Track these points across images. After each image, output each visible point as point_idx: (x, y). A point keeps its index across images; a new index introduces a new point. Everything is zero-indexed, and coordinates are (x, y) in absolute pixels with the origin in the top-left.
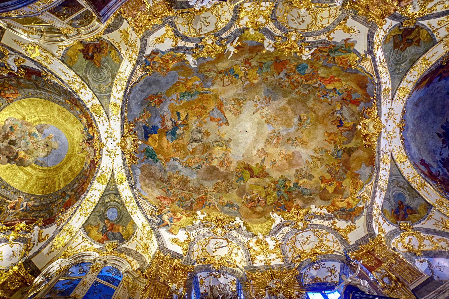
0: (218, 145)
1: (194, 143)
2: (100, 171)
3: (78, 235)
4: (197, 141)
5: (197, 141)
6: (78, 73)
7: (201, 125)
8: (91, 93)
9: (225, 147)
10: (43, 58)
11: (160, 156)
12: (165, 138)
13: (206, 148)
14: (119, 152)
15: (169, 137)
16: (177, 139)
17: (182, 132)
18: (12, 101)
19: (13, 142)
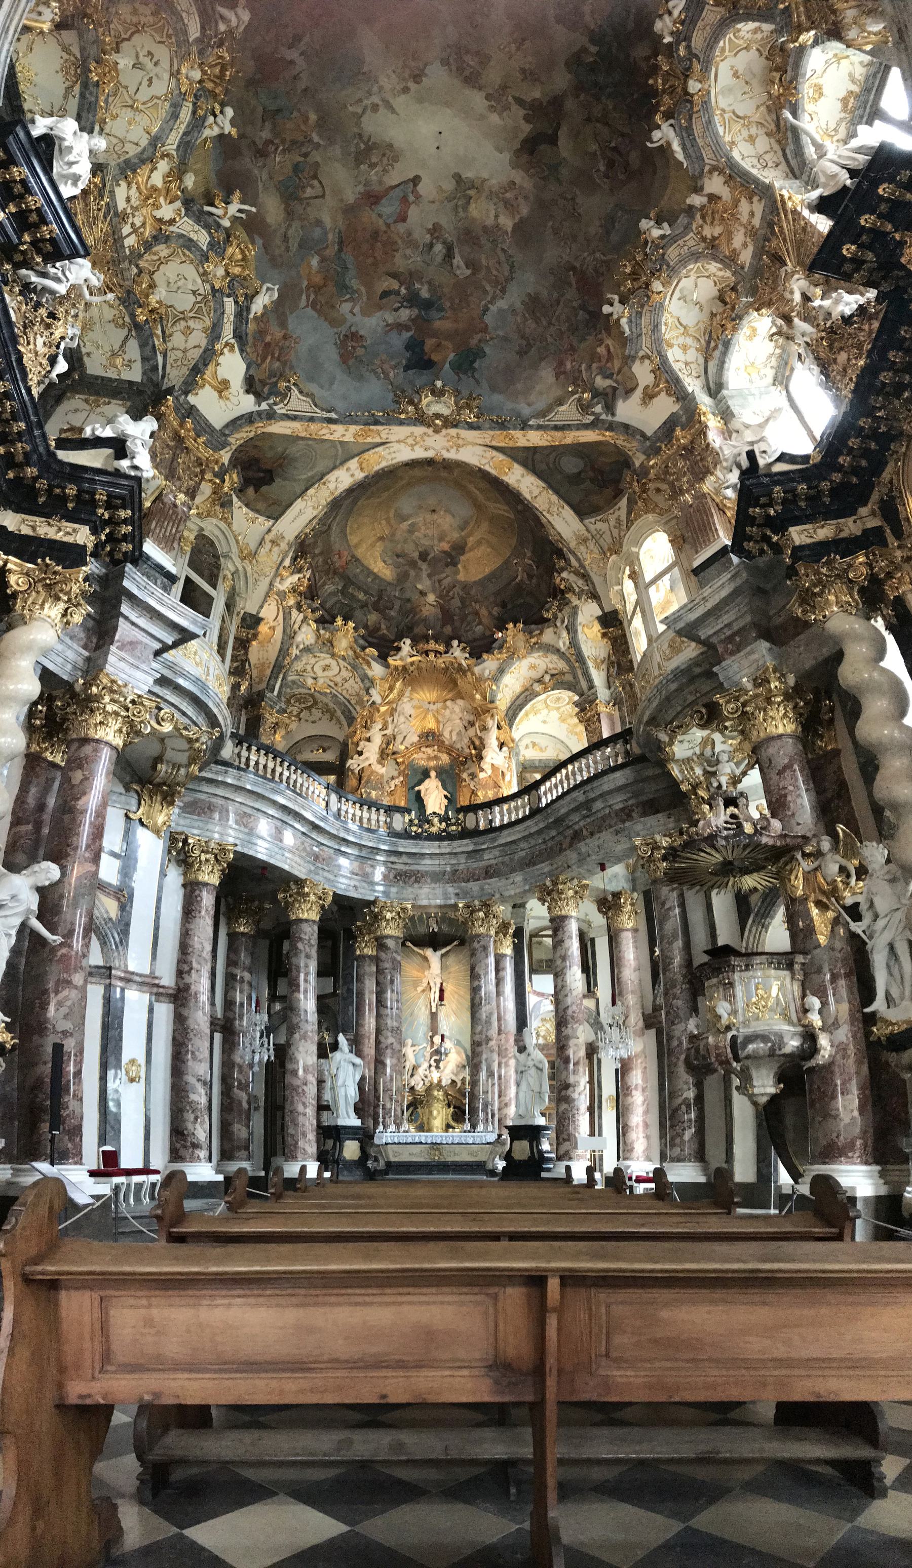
0: (465, 208)
1: (455, 262)
4: (449, 255)
5: (449, 255)
7: (411, 243)
9: (472, 192)
10: (276, 549)
11: (473, 342)
12: (437, 324)
13: (470, 236)
14: (453, 432)
15: (434, 314)
16: (440, 298)
17: (426, 287)
18: (353, 556)
19: (423, 556)
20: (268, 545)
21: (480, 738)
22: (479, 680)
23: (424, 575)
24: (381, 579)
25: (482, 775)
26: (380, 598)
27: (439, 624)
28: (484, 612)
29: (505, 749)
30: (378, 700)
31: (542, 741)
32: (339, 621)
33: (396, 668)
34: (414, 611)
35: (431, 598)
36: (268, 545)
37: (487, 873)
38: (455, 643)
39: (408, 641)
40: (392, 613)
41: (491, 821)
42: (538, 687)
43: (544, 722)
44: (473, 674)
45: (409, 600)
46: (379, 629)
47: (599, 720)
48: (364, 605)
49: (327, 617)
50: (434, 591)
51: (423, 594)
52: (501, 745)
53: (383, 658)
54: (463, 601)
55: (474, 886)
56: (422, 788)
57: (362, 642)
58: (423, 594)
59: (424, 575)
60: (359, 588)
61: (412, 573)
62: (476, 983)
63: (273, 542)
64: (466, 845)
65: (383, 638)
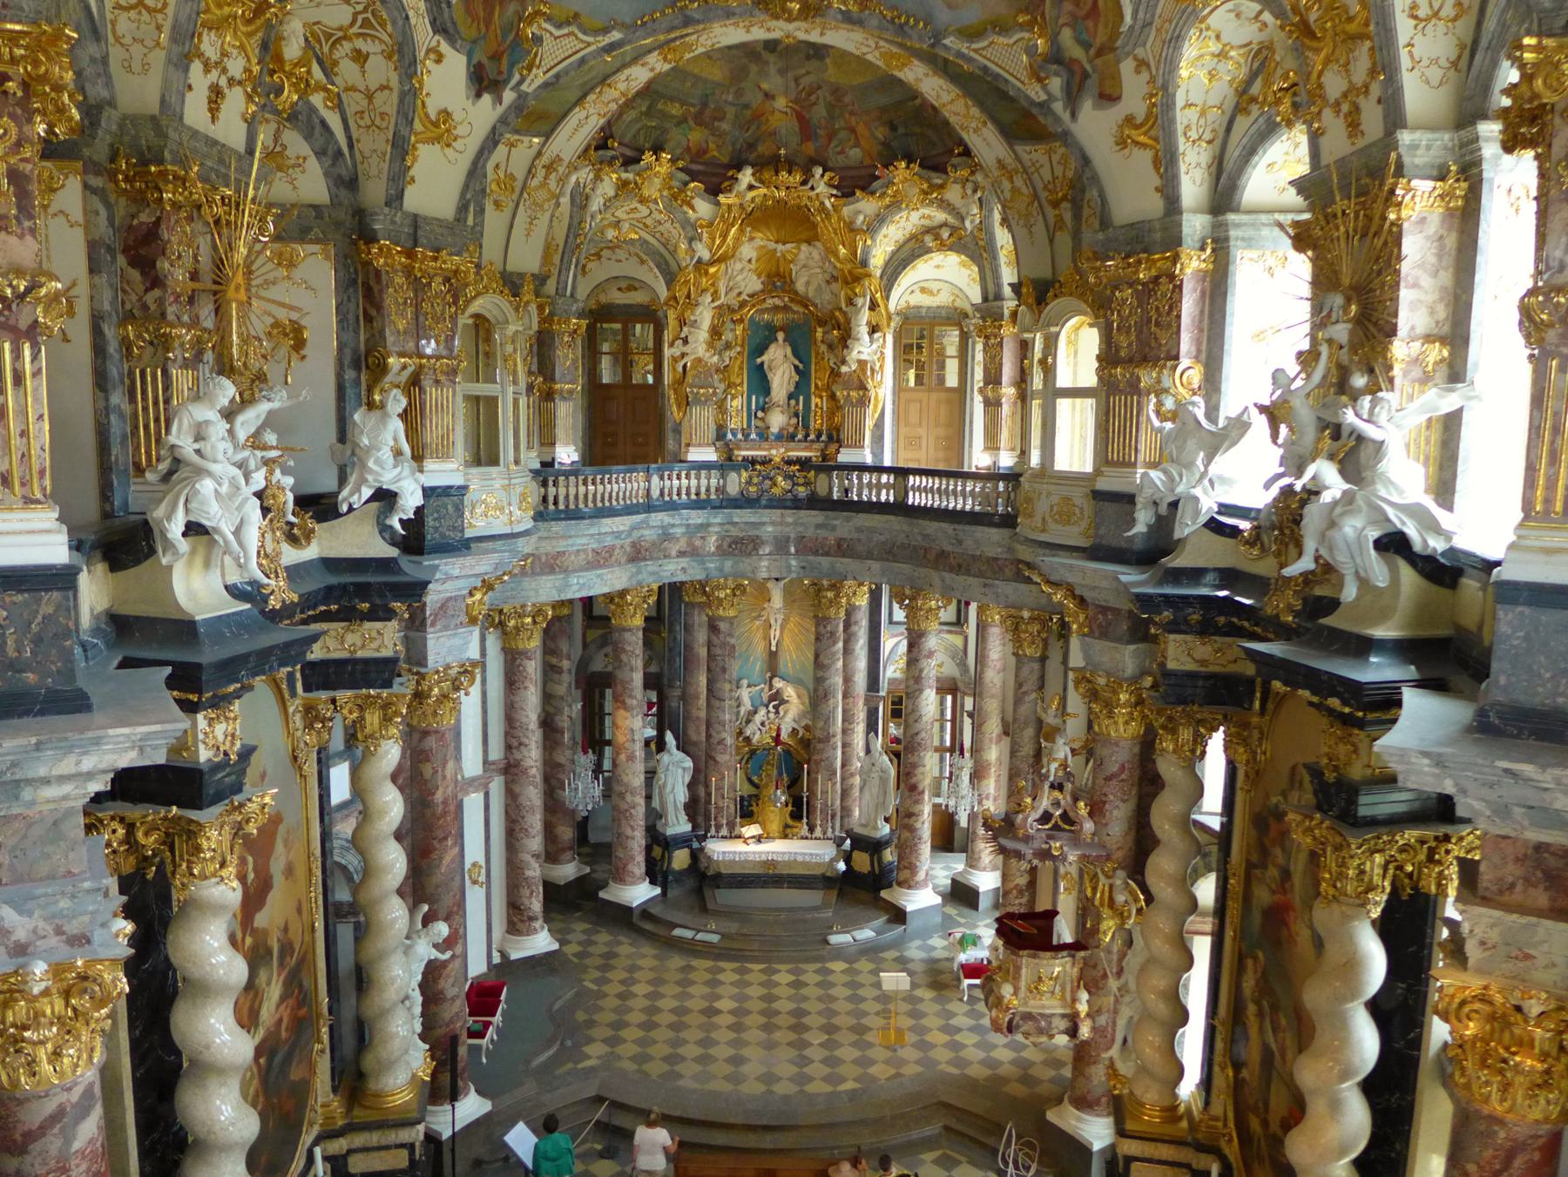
2: (869, 57)
3: (1025, 157)
6: (573, 99)
8: (627, 72)
20: (541, 173)
21: (845, 314)
22: (851, 228)
23: (772, 69)
24: (705, 81)
25: (844, 369)
26: (705, 105)
27: (795, 140)
28: (861, 129)
29: (876, 335)
30: (706, 255)
31: (934, 286)
32: (648, 157)
33: (729, 206)
34: (758, 117)
35: (781, 103)
36: (541, 173)
37: (839, 546)
38: (818, 171)
39: (748, 171)
40: (725, 126)
41: (846, 491)
42: (929, 241)
43: (938, 267)
44: (840, 219)
45: (746, 106)
46: (705, 152)
47: (1001, 344)
48: (682, 121)
49: (629, 153)
50: (786, 93)
51: (768, 96)
52: (874, 329)
53: (714, 191)
54: (831, 108)
55: (825, 562)
56: (765, 358)
57: (684, 177)
58: (768, 96)
59: (772, 69)
60: (672, 99)
61: (754, 68)
62: (820, 674)
63: (550, 168)
64: (813, 517)
65: (713, 163)
